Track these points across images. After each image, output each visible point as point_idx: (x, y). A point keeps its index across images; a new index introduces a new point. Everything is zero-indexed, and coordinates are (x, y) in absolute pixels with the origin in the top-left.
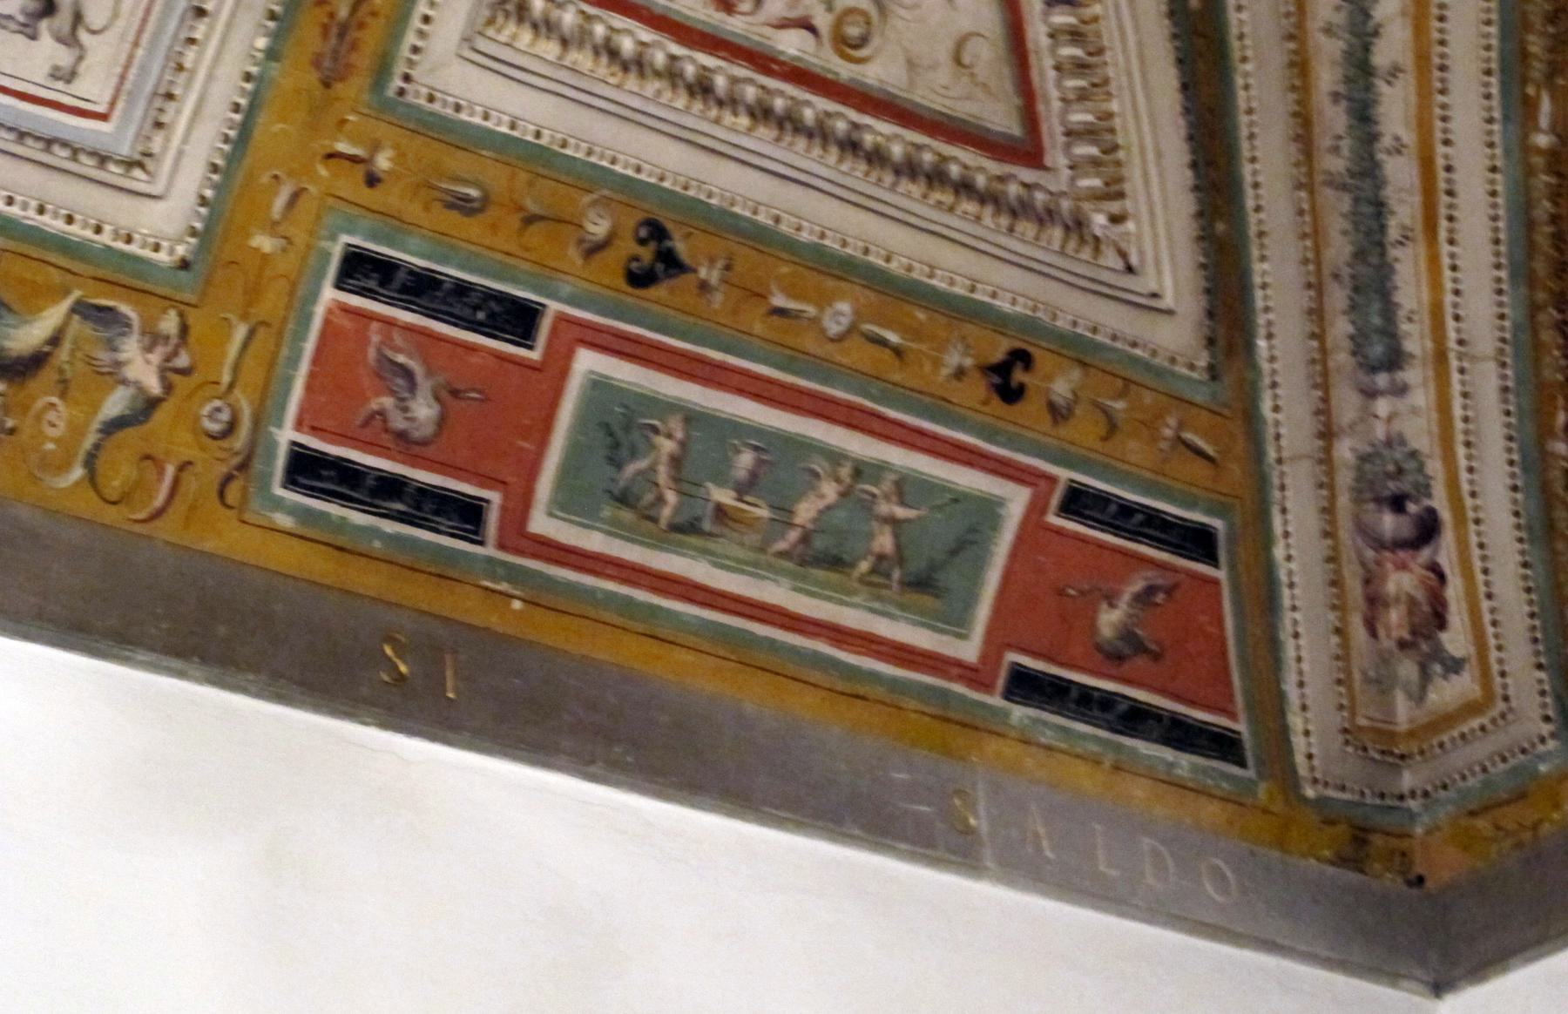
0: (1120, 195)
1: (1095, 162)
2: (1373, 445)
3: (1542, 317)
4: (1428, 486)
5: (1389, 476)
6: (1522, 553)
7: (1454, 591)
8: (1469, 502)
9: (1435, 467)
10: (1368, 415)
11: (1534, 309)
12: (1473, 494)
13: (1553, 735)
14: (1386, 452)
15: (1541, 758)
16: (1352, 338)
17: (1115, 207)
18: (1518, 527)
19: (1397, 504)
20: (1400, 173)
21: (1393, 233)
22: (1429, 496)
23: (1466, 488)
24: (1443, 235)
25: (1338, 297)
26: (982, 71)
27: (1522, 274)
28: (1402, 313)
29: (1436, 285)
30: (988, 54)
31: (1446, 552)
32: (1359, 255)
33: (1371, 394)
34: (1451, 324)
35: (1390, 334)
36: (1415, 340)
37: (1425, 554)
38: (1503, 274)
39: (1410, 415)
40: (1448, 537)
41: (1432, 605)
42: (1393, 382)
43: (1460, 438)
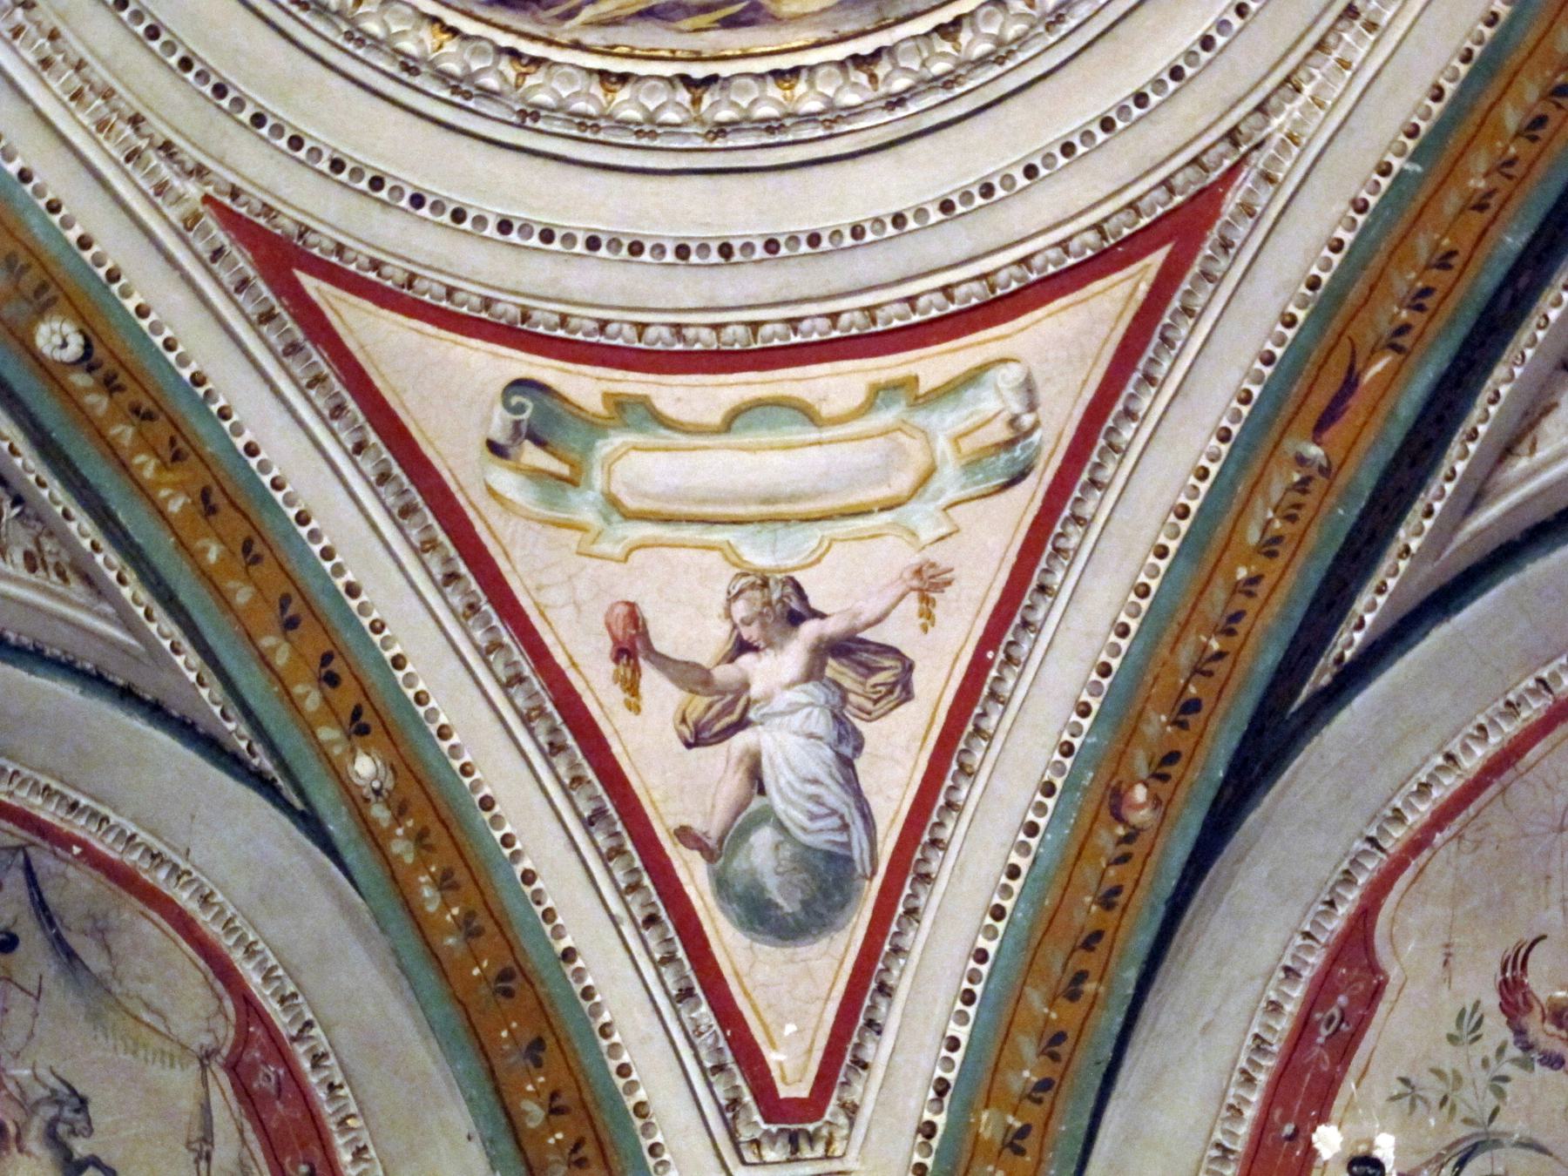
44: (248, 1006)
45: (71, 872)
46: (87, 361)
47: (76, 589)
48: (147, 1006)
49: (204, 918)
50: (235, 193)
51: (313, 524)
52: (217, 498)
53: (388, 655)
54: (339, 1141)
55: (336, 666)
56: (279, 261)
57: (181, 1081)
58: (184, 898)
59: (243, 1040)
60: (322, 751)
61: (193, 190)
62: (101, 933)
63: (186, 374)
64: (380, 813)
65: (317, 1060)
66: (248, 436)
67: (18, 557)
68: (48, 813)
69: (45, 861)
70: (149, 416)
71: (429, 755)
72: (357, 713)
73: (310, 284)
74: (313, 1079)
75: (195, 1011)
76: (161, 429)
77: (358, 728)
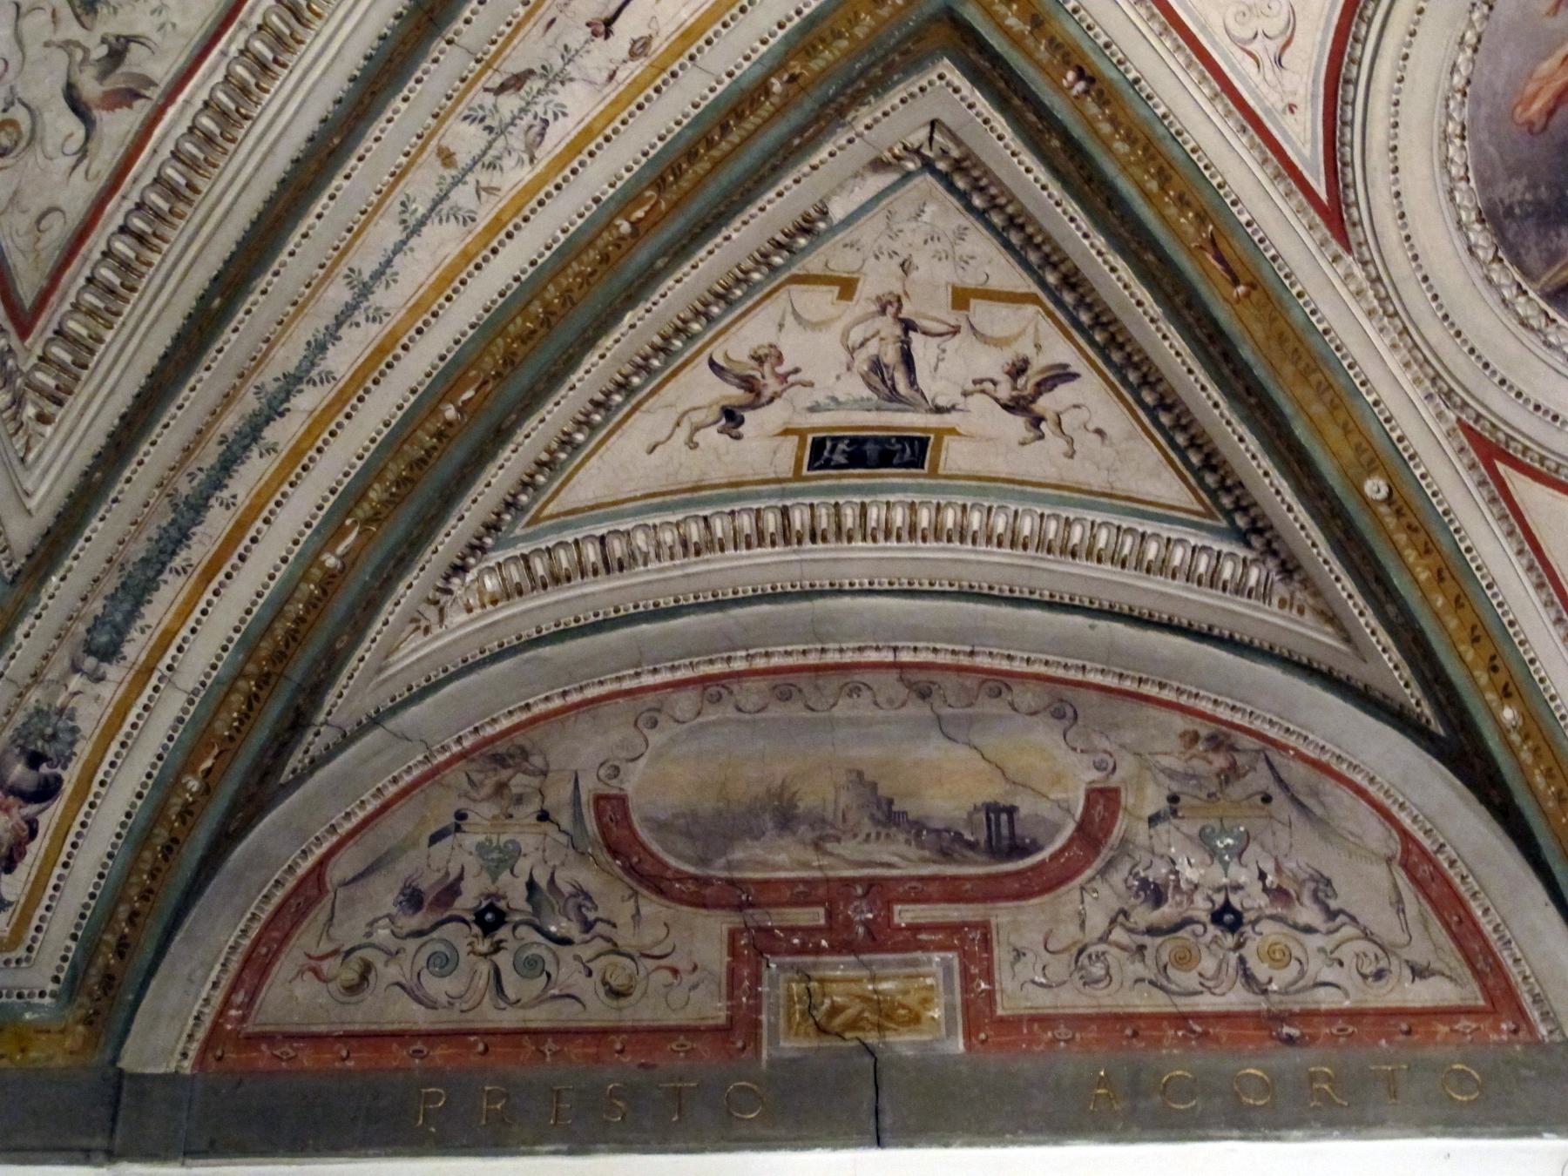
0: (60, 403)
1: (62, 367)
2: (50, 706)
3: (242, 684)
4: (69, 759)
5: (42, 736)
6: (114, 846)
7: (36, 849)
8: (95, 787)
9: (83, 749)
10: (62, 683)
11: (241, 674)
12: (102, 783)
13: (53, 995)
14: (54, 719)
15: (30, 1007)
16: (96, 618)
17: (50, 408)
18: (123, 825)
19: (34, 760)
20: (217, 522)
21: (178, 562)
22: (65, 767)
23: (100, 776)
24: (214, 585)
25: (110, 584)
26: (46, 239)
27: (249, 644)
28: (140, 623)
29: (183, 615)
30: (58, 231)
31: (50, 816)
32: (145, 561)
33: (76, 668)
34: (172, 651)
35: (120, 633)
36: (136, 647)
37: (31, 809)
38: (237, 637)
39: (91, 705)
40: (57, 807)
41: (11, 850)
42: (97, 668)
43: (120, 737)
44: (1405, 835)
45: (1292, 763)
46: (1389, 500)
47: (1308, 617)
48: (1351, 833)
49: (1372, 790)
50: (1479, 417)
51: (1495, 589)
52: (1446, 574)
53: (1526, 658)
54: (1473, 905)
55: (1497, 662)
56: (1490, 451)
57: (1379, 872)
58: (1358, 778)
59: (1406, 852)
60: (1487, 704)
61: (1451, 416)
62: (1315, 793)
63: (1440, 510)
64: (1515, 738)
65: (1452, 863)
66: (1468, 543)
67: (1275, 601)
68: (1272, 733)
69: (1276, 758)
70: (1416, 530)
71: (1546, 713)
72: (1506, 687)
73: (1501, 467)
74: (1451, 873)
75: (1376, 834)
76: (1422, 536)
77: (1506, 694)
